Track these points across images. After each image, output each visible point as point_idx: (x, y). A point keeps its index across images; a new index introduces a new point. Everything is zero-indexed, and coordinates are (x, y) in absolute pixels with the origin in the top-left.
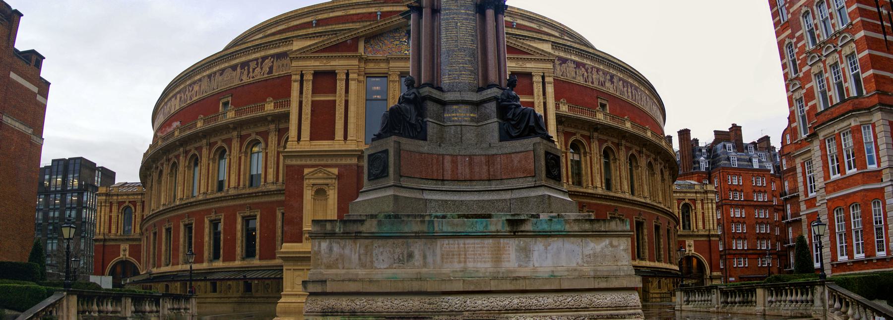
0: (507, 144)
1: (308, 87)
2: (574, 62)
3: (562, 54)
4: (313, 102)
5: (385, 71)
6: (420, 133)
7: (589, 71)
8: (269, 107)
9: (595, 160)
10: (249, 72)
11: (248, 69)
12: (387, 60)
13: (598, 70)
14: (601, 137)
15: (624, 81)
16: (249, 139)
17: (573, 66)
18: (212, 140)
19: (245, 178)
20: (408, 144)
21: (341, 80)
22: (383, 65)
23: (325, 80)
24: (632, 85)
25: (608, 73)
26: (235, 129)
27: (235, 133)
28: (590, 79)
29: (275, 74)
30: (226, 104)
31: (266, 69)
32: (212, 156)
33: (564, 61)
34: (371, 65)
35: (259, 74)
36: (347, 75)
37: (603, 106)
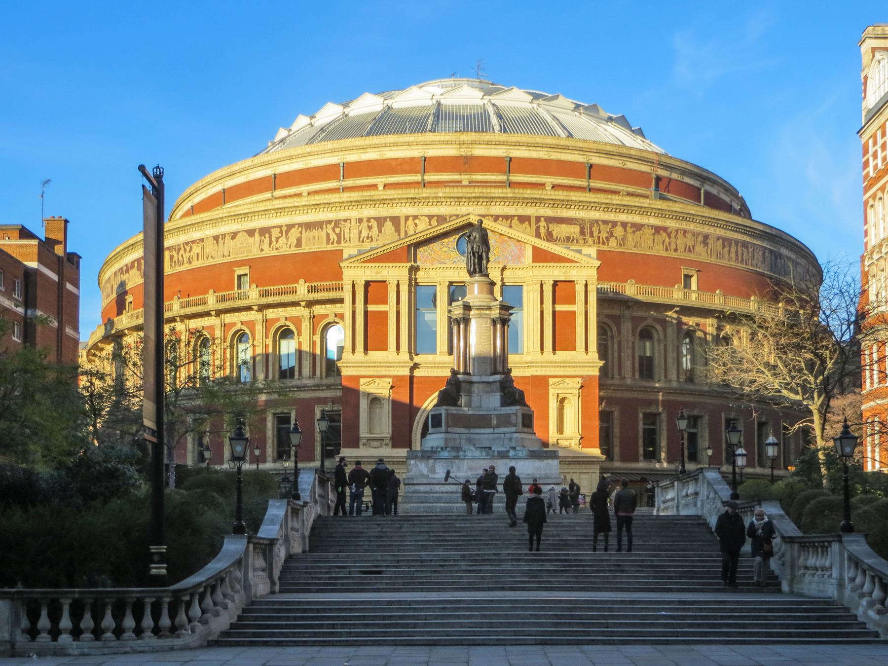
0: (503, 408)
3: (637, 219)
7: (673, 235)
9: (670, 348)
11: (270, 237)
13: (685, 232)
19: (274, 370)
20: (453, 410)
24: (737, 242)
25: (699, 234)
29: (305, 249)
31: (293, 240)
33: (638, 227)
35: (285, 247)
37: (688, 277)
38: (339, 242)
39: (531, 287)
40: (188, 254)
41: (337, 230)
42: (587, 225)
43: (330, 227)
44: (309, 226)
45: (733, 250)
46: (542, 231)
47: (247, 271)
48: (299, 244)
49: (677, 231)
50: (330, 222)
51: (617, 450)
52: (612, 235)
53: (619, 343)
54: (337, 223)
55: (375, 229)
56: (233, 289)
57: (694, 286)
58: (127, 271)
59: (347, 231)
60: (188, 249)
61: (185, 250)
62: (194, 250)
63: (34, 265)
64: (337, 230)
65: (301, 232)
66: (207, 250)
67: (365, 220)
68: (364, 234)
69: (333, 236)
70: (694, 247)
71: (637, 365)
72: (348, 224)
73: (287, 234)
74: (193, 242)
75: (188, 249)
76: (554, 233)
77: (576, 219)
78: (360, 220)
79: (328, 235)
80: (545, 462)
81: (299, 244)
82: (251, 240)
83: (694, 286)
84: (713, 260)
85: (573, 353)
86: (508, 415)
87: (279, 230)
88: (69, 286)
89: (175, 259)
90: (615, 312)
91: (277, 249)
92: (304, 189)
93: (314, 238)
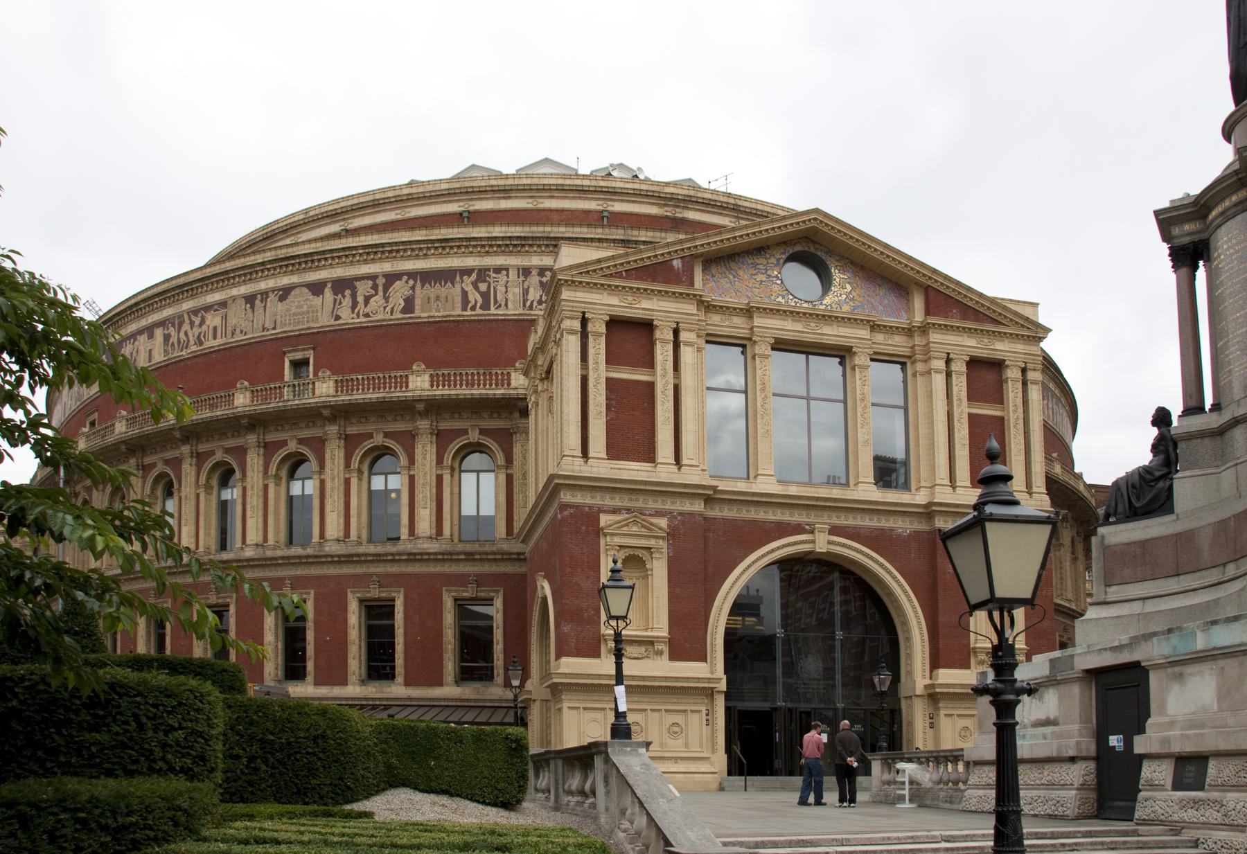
5: (744, 333)
8: (420, 383)
10: (355, 304)
11: (354, 296)
12: (748, 312)
16: (368, 444)
21: (664, 341)
22: (738, 321)
26: (333, 419)
27: (333, 429)
29: (421, 314)
34: (716, 318)
35: (382, 309)
36: (676, 332)
40: (196, 331)
43: (468, 280)
44: (427, 277)
48: (409, 306)
50: (467, 272)
54: (482, 273)
59: (501, 289)
60: (197, 321)
61: (192, 324)
62: (207, 322)
64: (483, 287)
65: (413, 288)
66: (232, 321)
67: (534, 272)
72: (502, 277)
73: (386, 289)
74: (208, 308)
75: (197, 321)
81: (409, 306)
82: (317, 301)
87: (370, 283)
89: (174, 339)
91: (367, 315)
93: (438, 298)
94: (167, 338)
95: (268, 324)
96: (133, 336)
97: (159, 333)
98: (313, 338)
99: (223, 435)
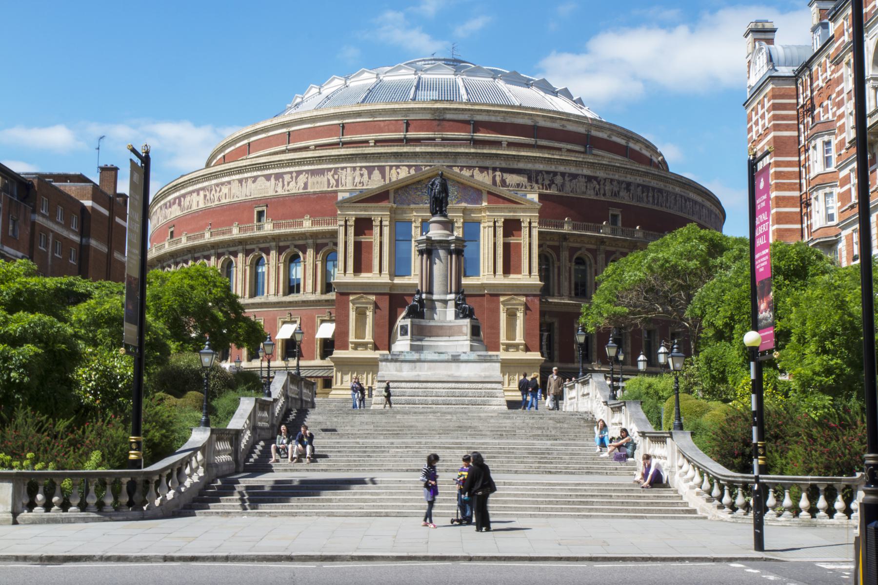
0: (457, 321)
1: (351, 231)
2: (585, 176)
3: (573, 170)
4: (355, 242)
6: (421, 316)
7: (602, 183)
8: (307, 225)
11: (283, 182)
13: (612, 180)
14: (609, 248)
15: (643, 186)
16: (288, 251)
17: (584, 180)
18: (248, 247)
20: (417, 320)
23: (363, 226)
24: (654, 189)
25: (623, 182)
28: (602, 192)
29: (310, 189)
30: (260, 214)
32: (248, 262)
33: (574, 176)
35: (295, 187)
37: (615, 217)
38: (337, 186)
39: (486, 225)
40: (218, 194)
41: (336, 177)
42: (534, 175)
44: (313, 173)
45: (650, 194)
46: (498, 179)
47: (265, 208)
49: (605, 179)
50: (330, 170)
51: (556, 353)
52: (553, 183)
53: (559, 268)
55: (366, 176)
56: (253, 222)
57: (620, 223)
58: (170, 207)
59: (344, 178)
60: (218, 189)
63: (88, 203)
64: (336, 177)
66: (233, 191)
67: (358, 169)
68: (357, 180)
69: (333, 182)
70: (619, 192)
71: (573, 286)
72: (344, 172)
74: (222, 184)
75: (218, 189)
76: (508, 181)
77: (525, 170)
78: (354, 168)
79: (329, 180)
80: (489, 364)
81: (305, 187)
82: (268, 183)
83: (620, 223)
84: (634, 203)
85: (519, 276)
86: (461, 326)
88: (118, 220)
89: (208, 197)
90: (556, 244)
92: (312, 143)
94: (205, 196)
95: (248, 194)
96: (191, 193)
97: (202, 193)
98: (267, 202)
99: (229, 246)
